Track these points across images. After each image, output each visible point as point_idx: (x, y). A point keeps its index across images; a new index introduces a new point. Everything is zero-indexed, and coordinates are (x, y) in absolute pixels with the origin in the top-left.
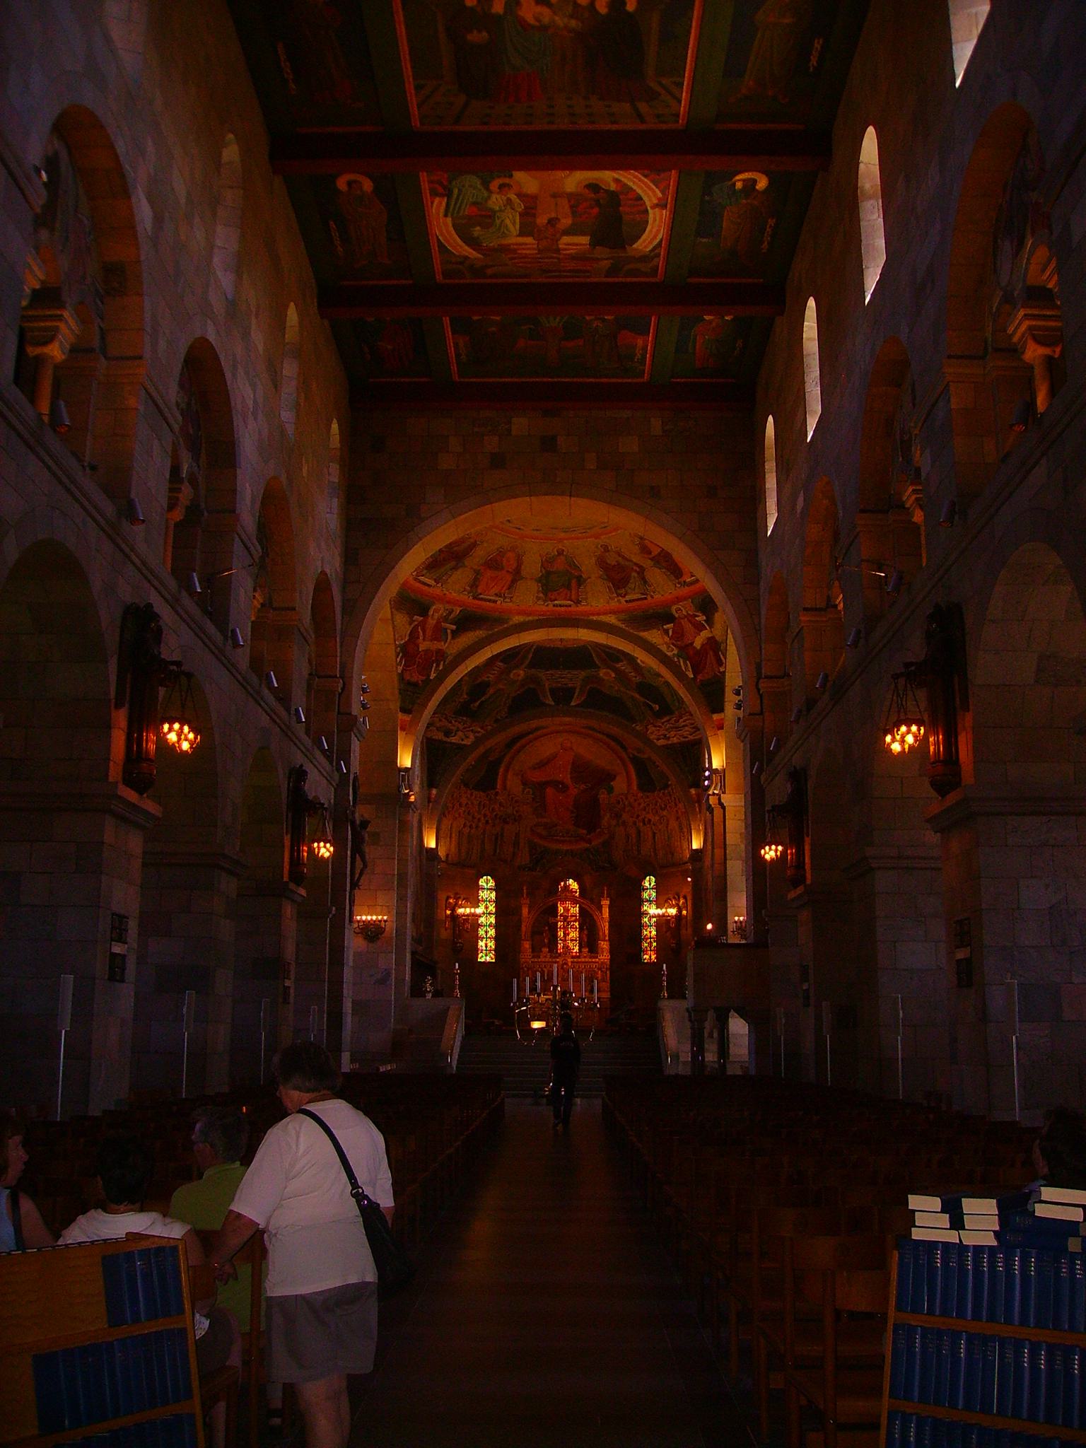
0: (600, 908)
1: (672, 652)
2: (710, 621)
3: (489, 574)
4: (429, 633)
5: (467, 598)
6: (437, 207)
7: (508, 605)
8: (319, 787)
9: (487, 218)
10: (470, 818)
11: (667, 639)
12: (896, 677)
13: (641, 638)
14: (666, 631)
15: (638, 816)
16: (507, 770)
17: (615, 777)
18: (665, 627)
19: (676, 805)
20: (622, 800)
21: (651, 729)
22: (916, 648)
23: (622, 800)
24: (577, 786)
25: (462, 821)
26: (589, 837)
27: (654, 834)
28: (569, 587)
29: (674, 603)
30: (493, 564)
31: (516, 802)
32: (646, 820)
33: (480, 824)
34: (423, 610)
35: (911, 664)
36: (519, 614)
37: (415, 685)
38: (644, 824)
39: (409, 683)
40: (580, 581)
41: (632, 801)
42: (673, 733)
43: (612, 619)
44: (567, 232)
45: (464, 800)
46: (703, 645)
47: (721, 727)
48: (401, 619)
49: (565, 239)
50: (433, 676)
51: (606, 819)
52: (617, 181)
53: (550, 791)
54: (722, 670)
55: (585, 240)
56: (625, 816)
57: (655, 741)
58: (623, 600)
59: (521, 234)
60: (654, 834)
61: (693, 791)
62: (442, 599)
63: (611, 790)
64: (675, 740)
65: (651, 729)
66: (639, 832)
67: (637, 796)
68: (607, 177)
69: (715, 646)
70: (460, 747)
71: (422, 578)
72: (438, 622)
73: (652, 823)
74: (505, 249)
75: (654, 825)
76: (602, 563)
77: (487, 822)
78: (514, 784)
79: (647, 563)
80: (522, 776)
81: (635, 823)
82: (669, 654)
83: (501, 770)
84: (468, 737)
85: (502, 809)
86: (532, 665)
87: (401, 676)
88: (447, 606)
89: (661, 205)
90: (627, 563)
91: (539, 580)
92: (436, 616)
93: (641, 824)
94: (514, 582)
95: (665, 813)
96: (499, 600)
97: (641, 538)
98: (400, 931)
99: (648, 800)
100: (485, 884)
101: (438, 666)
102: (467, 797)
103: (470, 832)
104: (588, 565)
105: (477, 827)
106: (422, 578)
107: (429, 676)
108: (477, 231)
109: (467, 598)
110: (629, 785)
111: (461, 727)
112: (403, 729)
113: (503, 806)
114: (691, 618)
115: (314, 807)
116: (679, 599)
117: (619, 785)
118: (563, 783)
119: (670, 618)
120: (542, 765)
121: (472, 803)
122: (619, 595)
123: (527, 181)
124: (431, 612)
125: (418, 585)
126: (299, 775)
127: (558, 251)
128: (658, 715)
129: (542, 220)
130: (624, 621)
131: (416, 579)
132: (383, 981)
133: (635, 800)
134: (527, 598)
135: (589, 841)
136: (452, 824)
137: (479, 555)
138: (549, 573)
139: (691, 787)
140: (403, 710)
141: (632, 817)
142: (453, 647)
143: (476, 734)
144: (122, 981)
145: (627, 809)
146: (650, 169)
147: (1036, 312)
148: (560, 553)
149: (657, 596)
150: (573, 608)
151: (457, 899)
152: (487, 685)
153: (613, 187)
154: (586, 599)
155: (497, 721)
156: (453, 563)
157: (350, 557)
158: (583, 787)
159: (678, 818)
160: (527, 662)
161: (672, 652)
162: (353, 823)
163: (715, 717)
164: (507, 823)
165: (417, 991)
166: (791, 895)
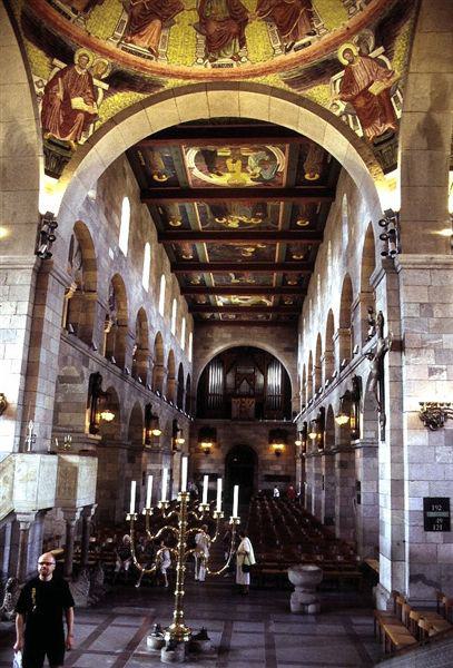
6: (282, 168)
9: (262, 163)
62: (336, 44)
68: (215, 180)
74: (256, 150)
108: (267, 158)
129: (239, 162)
146: (196, 180)
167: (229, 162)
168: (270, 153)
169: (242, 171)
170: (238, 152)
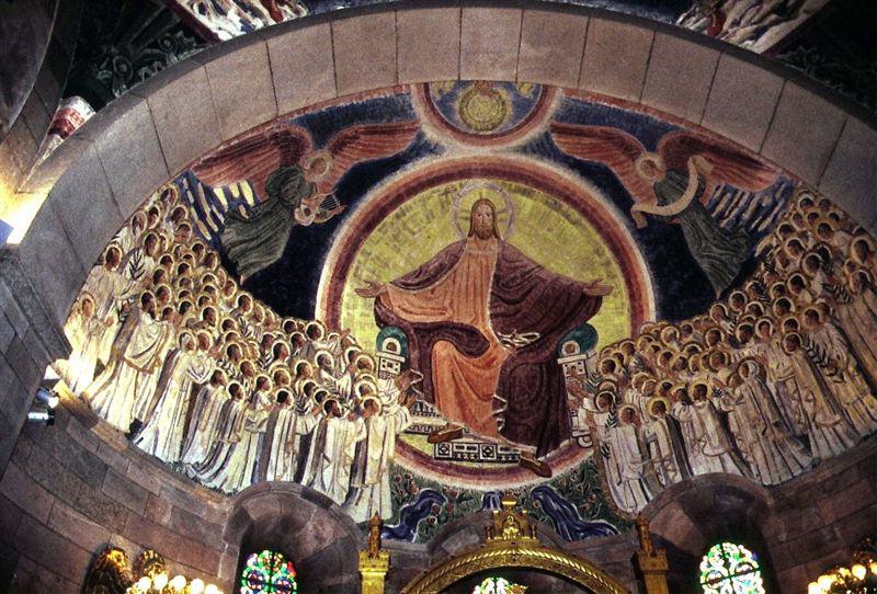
10: (236, 369)
15: (668, 387)
16: (340, 274)
17: (598, 301)
19: (785, 306)
20: (620, 357)
23: (620, 357)
24: (507, 337)
25: (211, 366)
26: (541, 459)
31: (362, 365)
32: (691, 391)
33: (263, 396)
38: (687, 402)
41: (645, 354)
45: (221, 311)
51: (582, 413)
53: (443, 350)
56: (631, 397)
57: (750, 42)
60: (723, 418)
63: (588, 339)
66: (674, 426)
67: (657, 338)
73: (710, 391)
75: (717, 394)
77: (283, 398)
78: (357, 317)
80: (378, 299)
81: (660, 408)
83: (326, 272)
84: (221, 12)
85: (325, 375)
93: (678, 406)
95: (746, 352)
99: (691, 338)
100: (262, 570)
102: (230, 304)
103: (228, 404)
105: (253, 400)
110: (637, 313)
113: (328, 370)
117: (610, 322)
118: (472, 332)
120: (422, 279)
121: (243, 328)
133: (657, 349)
135: (544, 471)
136: (171, 355)
141: (652, 394)
143: (248, 15)
145: (634, 378)
158: (521, 339)
159: (794, 343)
164: (337, 415)
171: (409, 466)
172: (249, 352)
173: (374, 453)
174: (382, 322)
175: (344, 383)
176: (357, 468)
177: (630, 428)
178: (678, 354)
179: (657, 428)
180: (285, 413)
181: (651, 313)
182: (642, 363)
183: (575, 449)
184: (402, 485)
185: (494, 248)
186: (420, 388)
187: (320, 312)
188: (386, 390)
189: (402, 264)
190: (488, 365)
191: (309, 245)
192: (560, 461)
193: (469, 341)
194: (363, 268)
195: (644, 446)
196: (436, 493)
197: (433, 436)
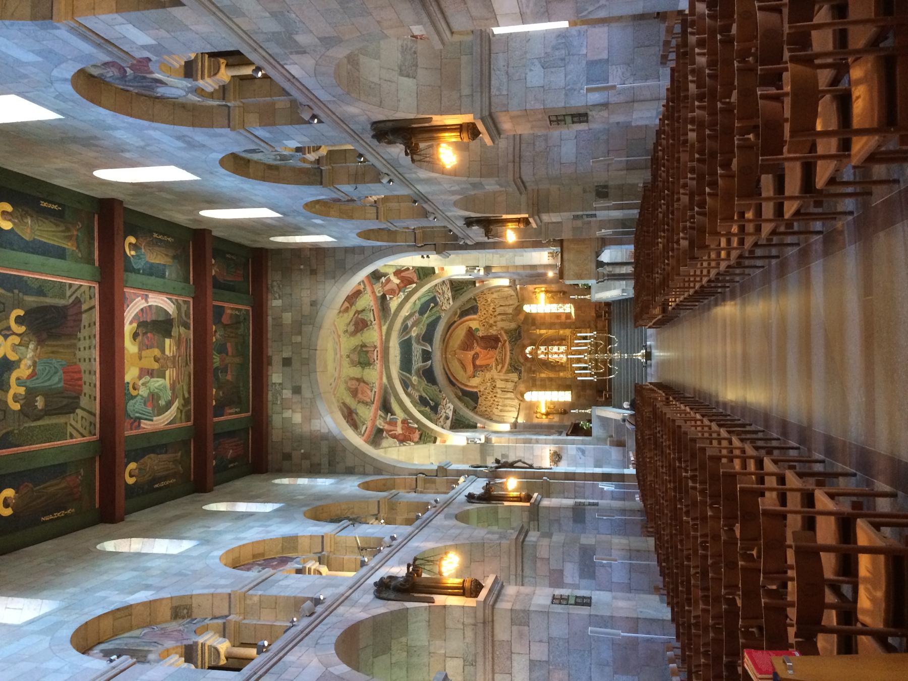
0: (541, 335)
1: (402, 296)
2: (385, 275)
3: (360, 395)
4: (392, 428)
5: (373, 407)
6: (147, 426)
7: (377, 384)
8: (478, 487)
9: (154, 397)
11: (395, 298)
12: (413, 160)
13: (395, 312)
14: (391, 298)
16: (467, 386)
17: (470, 328)
18: (388, 299)
21: (444, 308)
22: (397, 150)
27: (501, 306)
28: (367, 352)
29: (375, 295)
30: (354, 393)
34: (380, 431)
35: (406, 152)
36: (381, 378)
37: (421, 435)
39: (420, 438)
40: (363, 346)
42: (446, 296)
43: (384, 328)
44: (163, 351)
46: (398, 278)
47: (442, 269)
48: (385, 443)
49: (167, 352)
50: (416, 426)
52: (131, 323)
53: (478, 362)
54: (411, 268)
55: (167, 341)
56: (491, 321)
58: (374, 322)
59: (164, 377)
60: (501, 306)
61: (477, 285)
62: (374, 421)
63: (477, 330)
64: (450, 294)
65: (444, 308)
66: (499, 314)
68: (129, 328)
69: (398, 273)
70: (455, 411)
71: (362, 432)
72: (386, 423)
74: (173, 387)
76: (354, 333)
78: (475, 382)
79: (354, 309)
81: (495, 316)
82: (403, 297)
86: (410, 372)
87: (417, 443)
88: (378, 418)
89: (146, 298)
90: (354, 320)
91: (363, 368)
92: (383, 424)
94: (364, 382)
95: (489, 300)
96: (374, 390)
97: (340, 312)
98: (555, 442)
101: (410, 423)
104: (355, 341)
106: (362, 432)
107: (416, 428)
108: (162, 403)
109: (373, 407)
110: (474, 319)
111: (443, 411)
112: (444, 442)
114: (383, 285)
115: (488, 488)
116: (373, 292)
117: (474, 325)
119: (384, 297)
120: (464, 367)
122: (371, 325)
123: (131, 374)
124: (381, 427)
125: (366, 435)
126: (471, 498)
127: (174, 357)
128: (436, 304)
129: (156, 366)
130: (385, 322)
131: (363, 435)
132: (583, 452)
134: (373, 375)
135: (505, 341)
137: (349, 401)
138: (360, 363)
139: (475, 286)
140: (435, 442)
142: (400, 415)
144: (590, 598)
147: (200, 72)
148: (348, 356)
149: (372, 303)
150: (378, 349)
151: (537, 413)
152: (421, 397)
153: (135, 325)
154: (373, 342)
155: (440, 391)
156: (354, 415)
157: (350, 471)
158: (475, 345)
160: (408, 375)
161: (402, 296)
162: (497, 468)
163: (437, 272)
165: (588, 433)
166: (534, 225)
167: (156, 352)
168: (169, 405)
169: (141, 370)
170: (169, 364)
171: (504, 370)
172: (489, 404)
173: (503, 378)
174: (474, 377)
175: (489, 384)
176: (507, 381)
177: (498, 323)
178: (485, 312)
179: (499, 317)
180: (498, 396)
181: (475, 316)
182: (485, 319)
183: (500, 334)
184: (508, 372)
185: (458, 351)
186: (487, 367)
187: (475, 390)
188: (488, 375)
189: (462, 372)
190: (481, 352)
191: (466, 393)
192: (503, 337)
193: (475, 358)
194: (464, 381)
195: (503, 320)
196: (510, 364)
197: (497, 365)
